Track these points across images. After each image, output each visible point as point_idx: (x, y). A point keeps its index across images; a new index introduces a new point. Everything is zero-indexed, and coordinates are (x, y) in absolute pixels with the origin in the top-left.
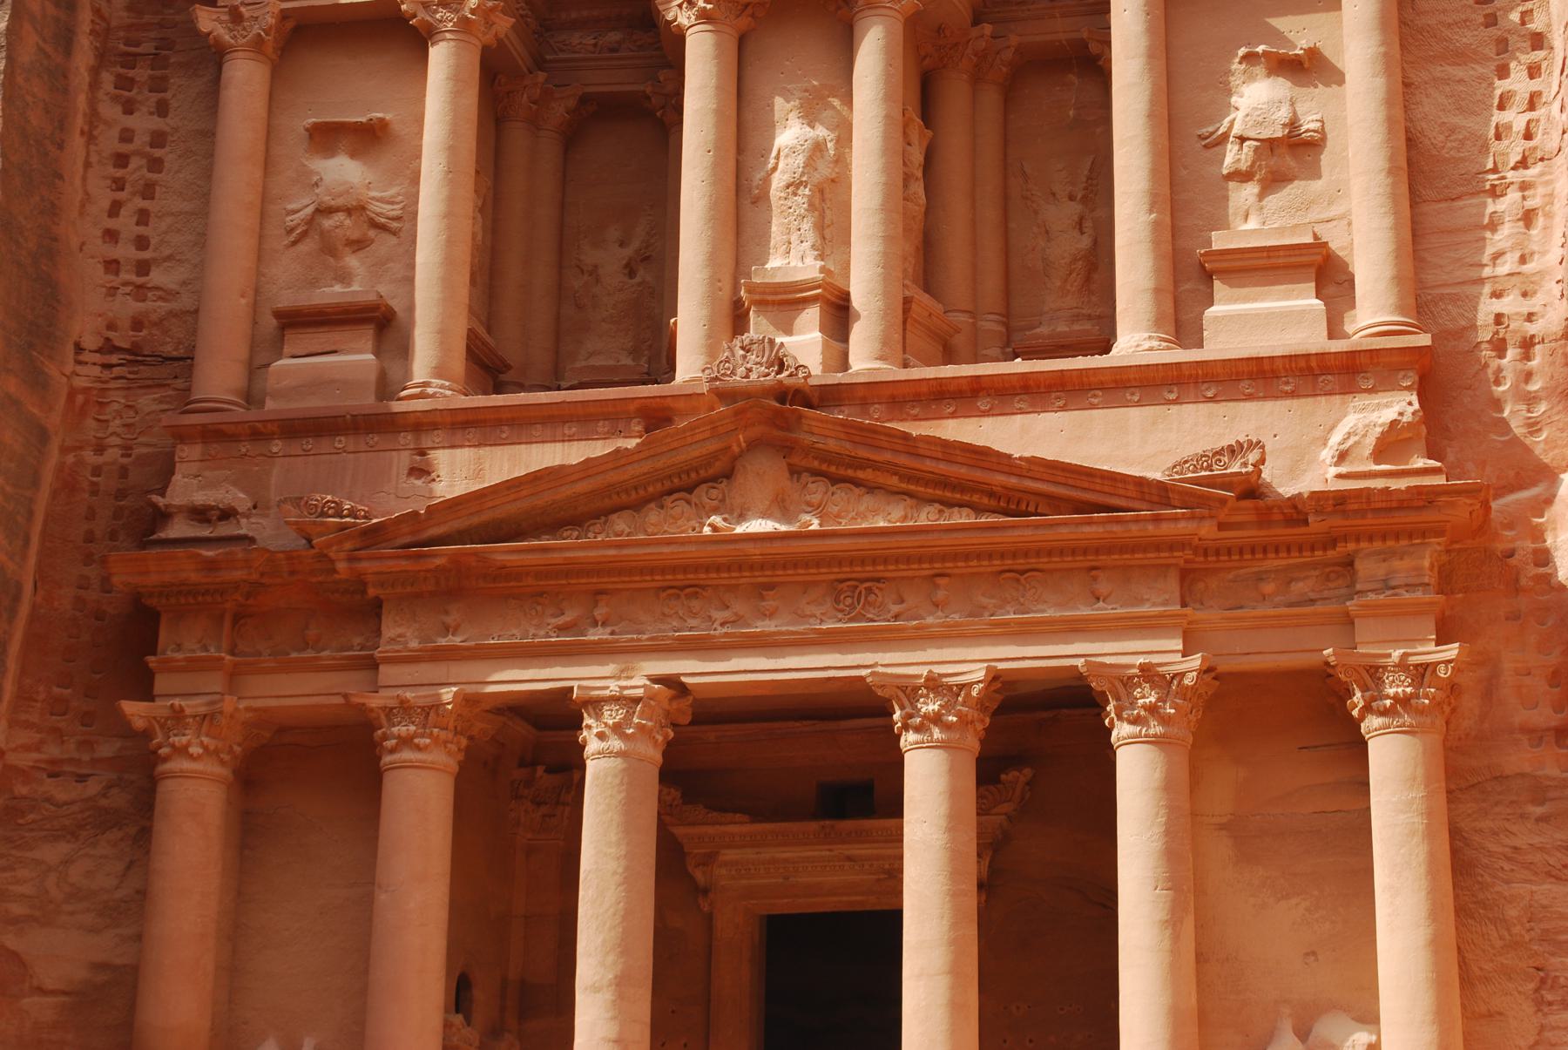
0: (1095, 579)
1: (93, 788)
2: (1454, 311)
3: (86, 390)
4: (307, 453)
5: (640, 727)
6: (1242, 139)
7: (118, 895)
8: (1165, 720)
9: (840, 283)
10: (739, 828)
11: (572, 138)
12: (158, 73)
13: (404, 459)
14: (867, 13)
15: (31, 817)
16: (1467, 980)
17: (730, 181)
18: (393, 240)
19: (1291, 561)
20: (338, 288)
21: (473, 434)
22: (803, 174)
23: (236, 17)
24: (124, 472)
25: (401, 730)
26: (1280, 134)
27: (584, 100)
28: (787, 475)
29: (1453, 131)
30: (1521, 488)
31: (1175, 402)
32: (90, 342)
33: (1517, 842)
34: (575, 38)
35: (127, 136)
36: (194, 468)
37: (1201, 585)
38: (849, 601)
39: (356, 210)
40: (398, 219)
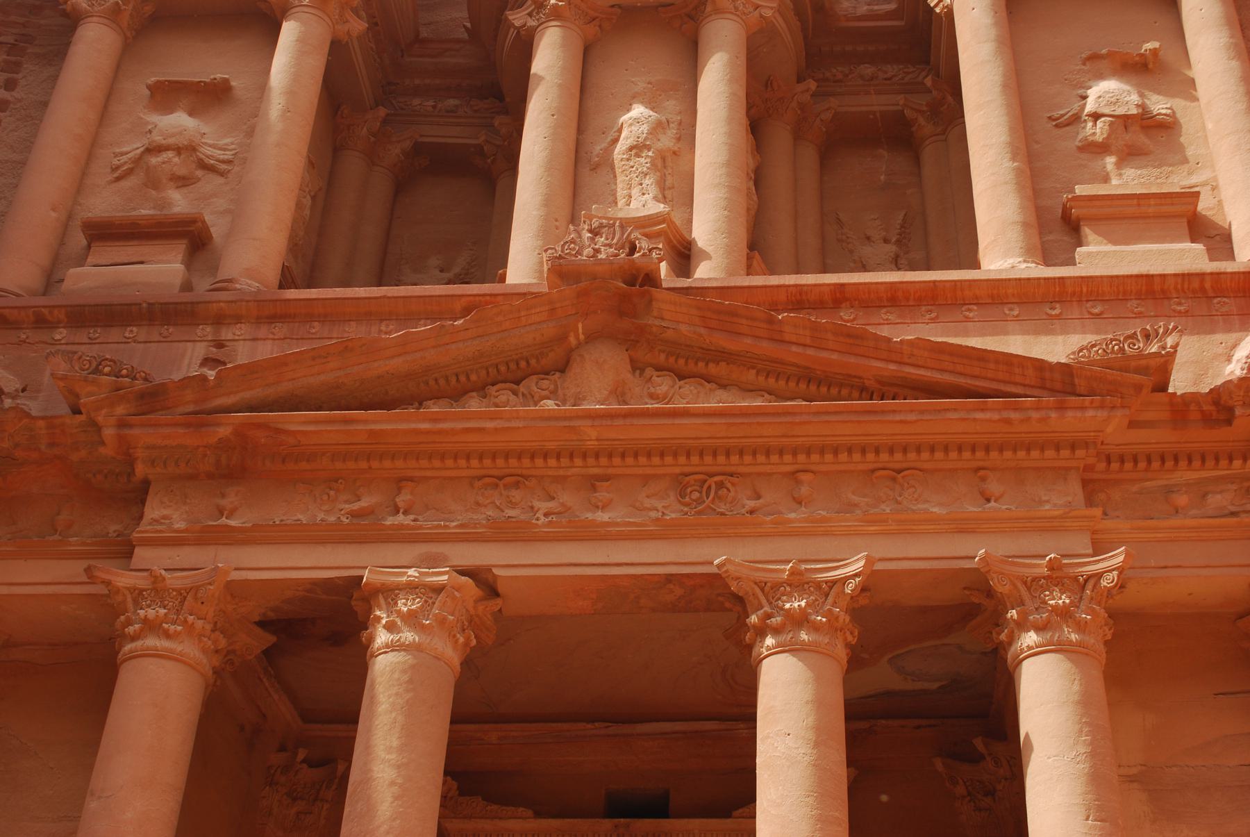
0: (983, 479)
6: (1096, 116)
8: (1080, 627)
11: (402, 184)
12: (13, 59)
13: (200, 350)
14: (713, 17)
17: (573, 147)
18: (221, 180)
19: (1204, 474)
21: (280, 329)
22: (646, 139)
25: (151, 613)
26: (1134, 111)
28: (629, 368)
31: (1058, 317)
34: (416, 102)
37: (1102, 496)
38: (696, 495)
39: (187, 149)
40: (229, 162)
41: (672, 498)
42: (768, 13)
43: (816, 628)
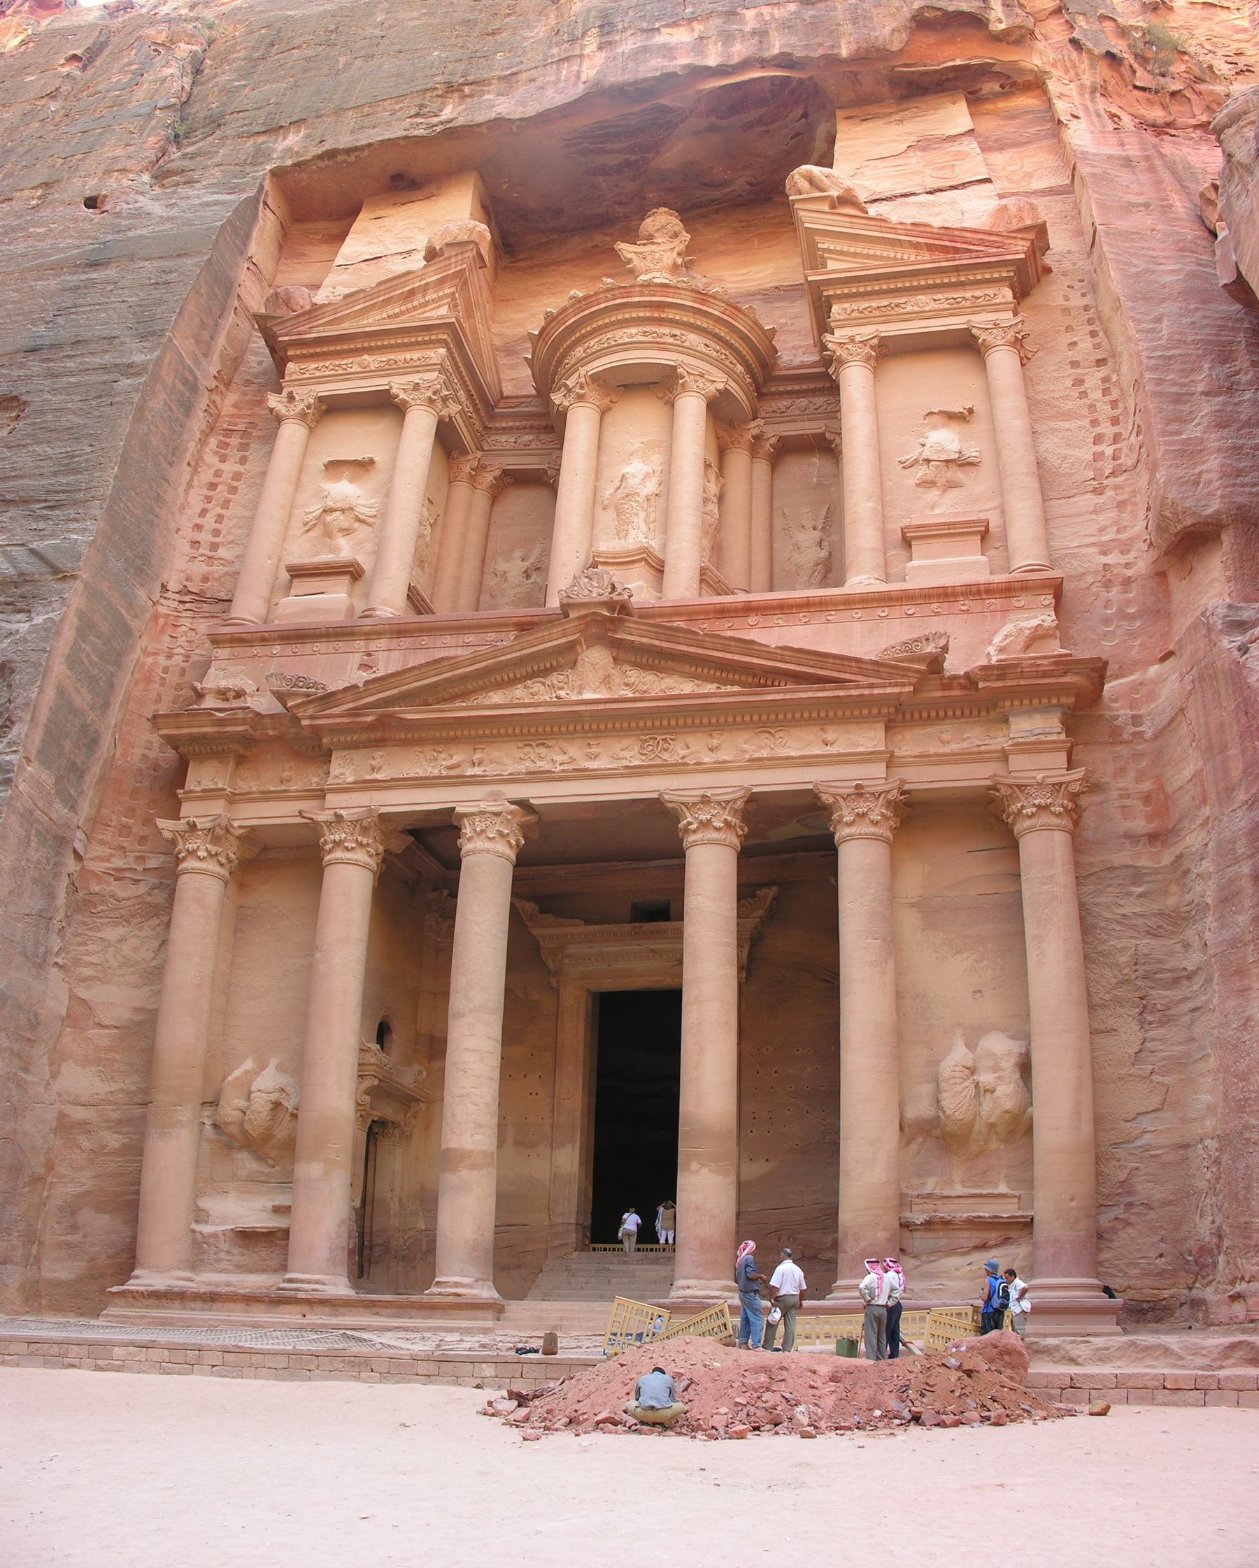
2: (1075, 563)
6: (928, 461)
9: (659, 555)
10: (577, 929)
16: (1092, 1008)
21: (406, 642)
29: (1065, 458)
30: (1123, 676)
42: (721, 386)
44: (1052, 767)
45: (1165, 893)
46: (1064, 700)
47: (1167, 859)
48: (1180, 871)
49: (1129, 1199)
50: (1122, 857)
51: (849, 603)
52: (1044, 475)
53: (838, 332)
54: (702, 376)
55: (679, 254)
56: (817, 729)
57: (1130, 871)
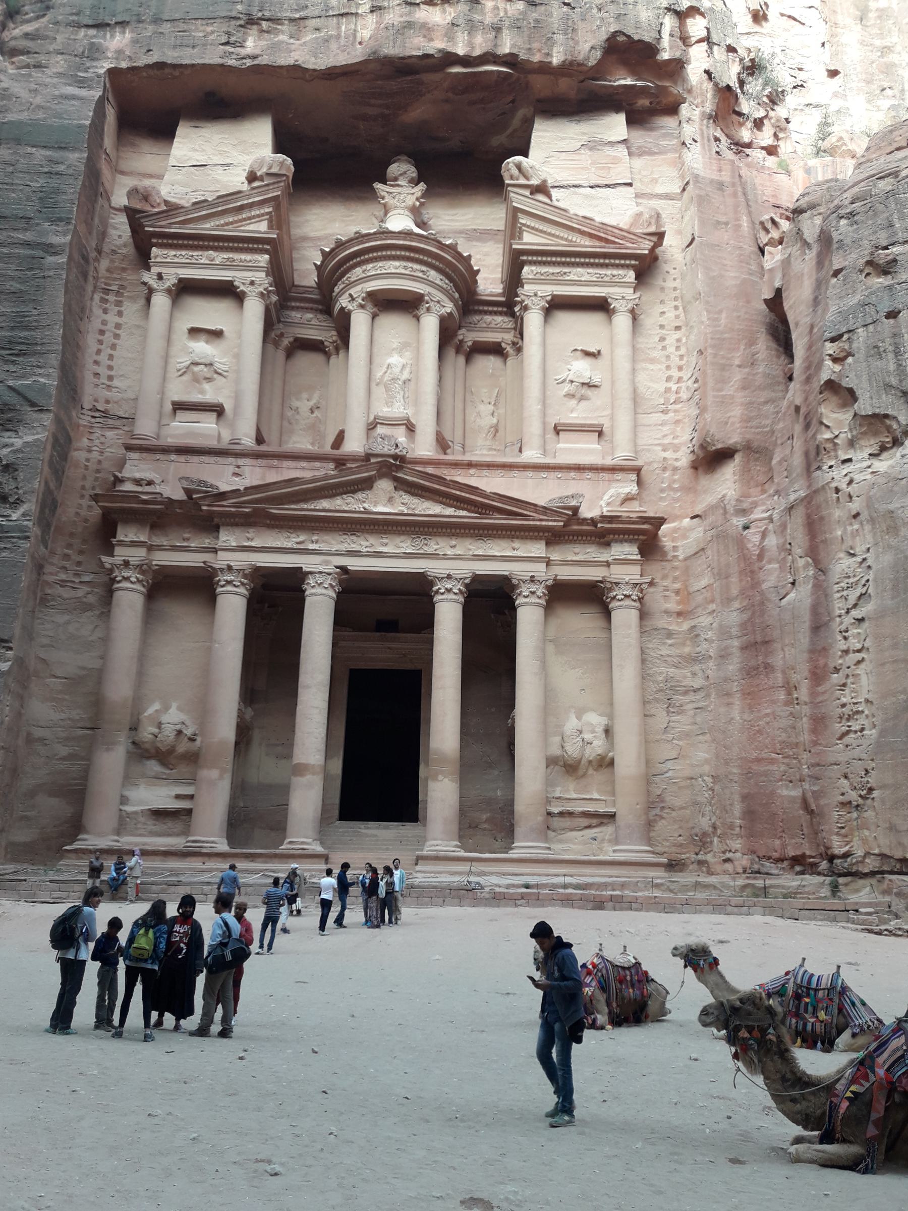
1: (80, 593)
3: (85, 426)
4: (187, 462)
5: (330, 585)
6: (572, 382)
7: (90, 639)
8: (539, 598)
15: (52, 603)
16: (645, 703)
20: (200, 396)
23: (160, 277)
24: (100, 462)
27: (296, 340)
32: (87, 406)
33: (663, 653)
35: (104, 323)
36: (136, 463)
37: (552, 548)
41: (409, 542)
42: (449, 310)
43: (456, 594)
44: (631, 574)
45: (684, 644)
46: (641, 537)
47: (686, 626)
48: (694, 634)
49: (662, 805)
50: (662, 622)
51: (525, 467)
52: (636, 399)
53: (526, 287)
54: (438, 302)
55: (417, 199)
56: (509, 540)
57: (665, 632)
